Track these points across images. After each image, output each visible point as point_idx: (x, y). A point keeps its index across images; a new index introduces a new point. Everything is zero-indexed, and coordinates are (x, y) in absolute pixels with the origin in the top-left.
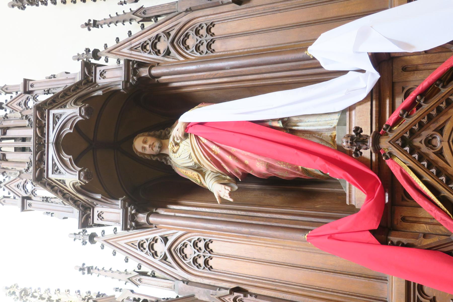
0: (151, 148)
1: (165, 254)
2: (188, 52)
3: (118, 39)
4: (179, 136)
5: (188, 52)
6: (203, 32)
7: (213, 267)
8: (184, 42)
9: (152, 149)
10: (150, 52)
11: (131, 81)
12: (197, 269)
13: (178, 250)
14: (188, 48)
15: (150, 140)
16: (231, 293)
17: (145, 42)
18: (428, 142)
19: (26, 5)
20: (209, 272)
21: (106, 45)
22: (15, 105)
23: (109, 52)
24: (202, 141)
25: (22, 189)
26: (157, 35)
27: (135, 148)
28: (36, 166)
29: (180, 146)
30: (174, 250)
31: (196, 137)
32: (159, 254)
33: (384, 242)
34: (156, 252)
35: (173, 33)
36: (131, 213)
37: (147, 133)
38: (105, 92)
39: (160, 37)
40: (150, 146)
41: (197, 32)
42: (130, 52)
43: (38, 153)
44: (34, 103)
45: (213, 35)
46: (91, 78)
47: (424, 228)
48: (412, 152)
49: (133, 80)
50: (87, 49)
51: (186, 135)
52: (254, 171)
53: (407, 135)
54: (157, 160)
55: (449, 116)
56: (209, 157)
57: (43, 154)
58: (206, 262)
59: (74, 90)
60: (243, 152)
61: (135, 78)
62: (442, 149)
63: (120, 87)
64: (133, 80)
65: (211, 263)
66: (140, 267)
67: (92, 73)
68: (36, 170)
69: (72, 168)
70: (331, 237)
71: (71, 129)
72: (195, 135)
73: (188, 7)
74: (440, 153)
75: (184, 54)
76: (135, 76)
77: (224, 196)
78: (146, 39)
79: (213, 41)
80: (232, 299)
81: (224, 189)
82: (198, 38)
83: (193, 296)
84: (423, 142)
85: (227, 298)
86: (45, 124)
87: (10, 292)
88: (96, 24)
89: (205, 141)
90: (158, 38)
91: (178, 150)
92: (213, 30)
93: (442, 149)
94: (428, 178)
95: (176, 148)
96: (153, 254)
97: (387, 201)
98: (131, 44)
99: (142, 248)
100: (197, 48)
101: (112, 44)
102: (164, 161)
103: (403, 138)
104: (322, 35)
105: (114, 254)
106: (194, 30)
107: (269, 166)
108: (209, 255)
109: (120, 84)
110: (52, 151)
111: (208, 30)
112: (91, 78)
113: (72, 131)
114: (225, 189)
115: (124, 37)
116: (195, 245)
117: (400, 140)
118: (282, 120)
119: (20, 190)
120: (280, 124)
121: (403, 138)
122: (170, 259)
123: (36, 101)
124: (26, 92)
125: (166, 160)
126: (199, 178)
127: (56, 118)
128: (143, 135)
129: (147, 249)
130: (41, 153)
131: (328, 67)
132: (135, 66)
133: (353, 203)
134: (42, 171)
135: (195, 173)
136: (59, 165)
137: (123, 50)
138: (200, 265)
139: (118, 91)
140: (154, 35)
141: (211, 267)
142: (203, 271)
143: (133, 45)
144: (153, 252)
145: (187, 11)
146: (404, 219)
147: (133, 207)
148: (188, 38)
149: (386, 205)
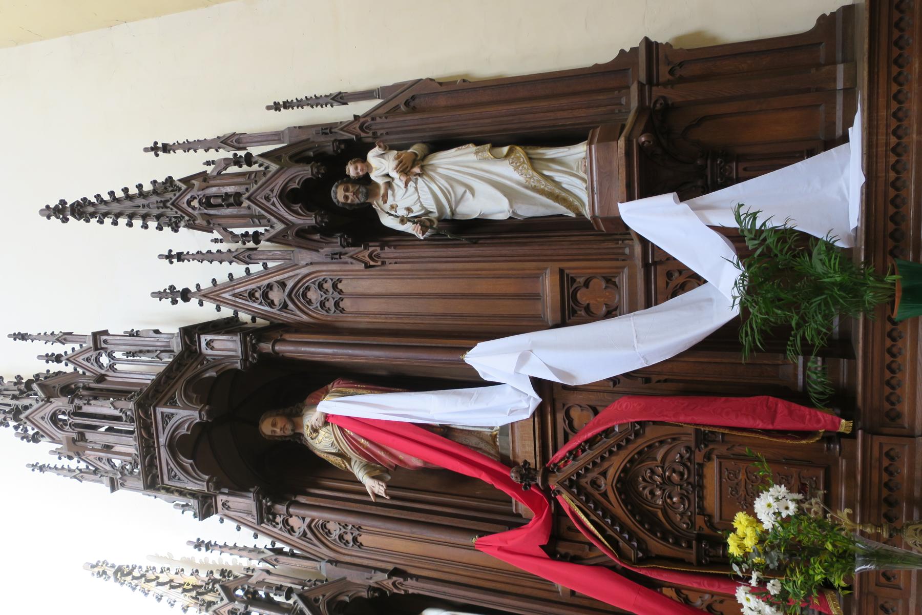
1: (304, 530)
2: (311, 307)
3: (214, 281)
5: (311, 307)
6: (328, 286)
7: (363, 544)
8: (304, 295)
10: (261, 302)
11: (250, 359)
12: (344, 546)
13: (320, 526)
14: (310, 302)
15: (280, 422)
16: (389, 578)
17: (253, 289)
18: (594, 483)
19: (69, 217)
20: (360, 550)
21: (198, 286)
22: (80, 359)
23: (205, 296)
24: (347, 433)
25: (107, 463)
26: (269, 284)
27: (262, 432)
28: (146, 472)
29: (319, 433)
30: (315, 526)
32: (296, 529)
34: (292, 528)
35: (290, 284)
36: (266, 505)
38: (219, 373)
39: (272, 285)
40: (281, 430)
41: (320, 286)
42: (233, 299)
43: (146, 457)
44: (110, 361)
45: (341, 292)
46: (194, 348)
48: (579, 494)
49: (253, 358)
51: (326, 423)
52: (409, 466)
53: (574, 478)
56: (358, 451)
57: (153, 458)
58: (355, 540)
59: (177, 369)
61: (255, 355)
62: (606, 490)
63: (238, 366)
64: (253, 358)
65: (360, 539)
66: (273, 544)
67: (196, 341)
69: (194, 474)
71: (187, 430)
72: (338, 426)
73: (309, 261)
74: (605, 495)
75: (304, 309)
76: (255, 353)
77: (378, 492)
78: (254, 286)
80: (390, 584)
81: (377, 486)
82: (322, 293)
83: (344, 578)
84: (589, 482)
86: (152, 423)
87: (99, 572)
88: (180, 257)
90: (270, 287)
91: (317, 436)
92: (340, 286)
93: (606, 490)
95: (315, 435)
96: (288, 530)
98: (234, 289)
99: (274, 524)
100: (322, 304)
101: (206, 285)
103: (570, 480)
104: (479, 344)
105: (239, 529)
106: (317, 283)
108: (357, 532)
109: (237, 363)
110: (164, 454)
111: (335, 286)
112: (194, 348)
113: (189, 433)
114: (379, 485)
115: (222, 279)
117: (567, 481)
119: (104, 463)
122: (309, 535)
123: (113, 359)
124: (96, 347)
125: (301, 440)
126: (344, 463)
127: (167, 418)
128: (271, 416)
129: (281, 525)
130: (151, 457)
131: (487, 379)
132: (254, 342)
133: (520, 512)
135: (339, 459)
136: (177, 470)
137: (223, 295)
138: (347, 541)
139: (236, 370)
140: (266, 282)
141: (361, 544)
142: (352, 548)
143: (237, 291)
144: (289, 527)
145: (307, 265)
147: (268, 499)
148: (309, 290)
149: (553, 515)
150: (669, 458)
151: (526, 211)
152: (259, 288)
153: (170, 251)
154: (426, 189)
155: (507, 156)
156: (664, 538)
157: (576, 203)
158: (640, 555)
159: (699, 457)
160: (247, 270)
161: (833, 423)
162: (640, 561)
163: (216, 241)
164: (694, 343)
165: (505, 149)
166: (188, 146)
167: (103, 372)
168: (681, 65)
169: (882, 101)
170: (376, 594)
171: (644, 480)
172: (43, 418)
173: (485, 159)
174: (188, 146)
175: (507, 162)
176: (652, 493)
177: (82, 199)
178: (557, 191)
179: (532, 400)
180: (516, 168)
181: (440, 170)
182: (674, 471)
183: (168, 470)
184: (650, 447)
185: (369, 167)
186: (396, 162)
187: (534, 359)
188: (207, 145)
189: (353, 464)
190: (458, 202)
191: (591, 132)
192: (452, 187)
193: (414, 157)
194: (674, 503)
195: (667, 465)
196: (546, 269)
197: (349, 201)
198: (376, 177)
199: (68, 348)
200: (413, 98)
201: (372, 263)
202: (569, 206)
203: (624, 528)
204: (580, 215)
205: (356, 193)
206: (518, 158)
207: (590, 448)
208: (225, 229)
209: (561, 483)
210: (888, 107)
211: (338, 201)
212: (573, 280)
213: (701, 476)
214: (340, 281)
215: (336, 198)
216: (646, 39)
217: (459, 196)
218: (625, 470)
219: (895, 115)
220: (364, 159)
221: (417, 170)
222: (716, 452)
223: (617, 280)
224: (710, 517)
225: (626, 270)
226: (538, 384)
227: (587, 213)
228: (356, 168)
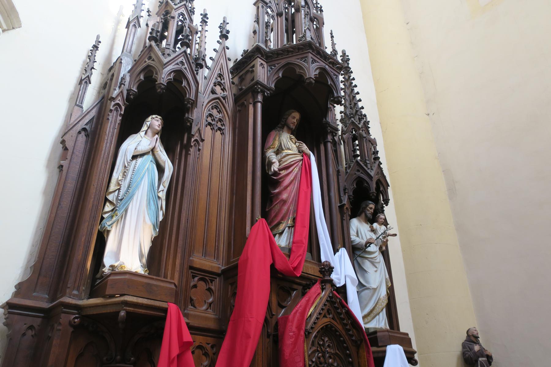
0: (293, 122)
4: (303, 148)
9: (293, 123)
12: (206, 115)
28: (317, 48)
37: (299, 123)
43: (323, 53)
50: (229, 32)
55: (339, 324)
57: (321, 57)
58: (210, 124)
68: (316, 47)
80: (197, 138)
85: (197, 134)
91: (292, 142)
97: (279, 275)
107: (284, 202)
134: (313, 50)
177: (351, 71)
211: (370, 204)
215: (372, 204)
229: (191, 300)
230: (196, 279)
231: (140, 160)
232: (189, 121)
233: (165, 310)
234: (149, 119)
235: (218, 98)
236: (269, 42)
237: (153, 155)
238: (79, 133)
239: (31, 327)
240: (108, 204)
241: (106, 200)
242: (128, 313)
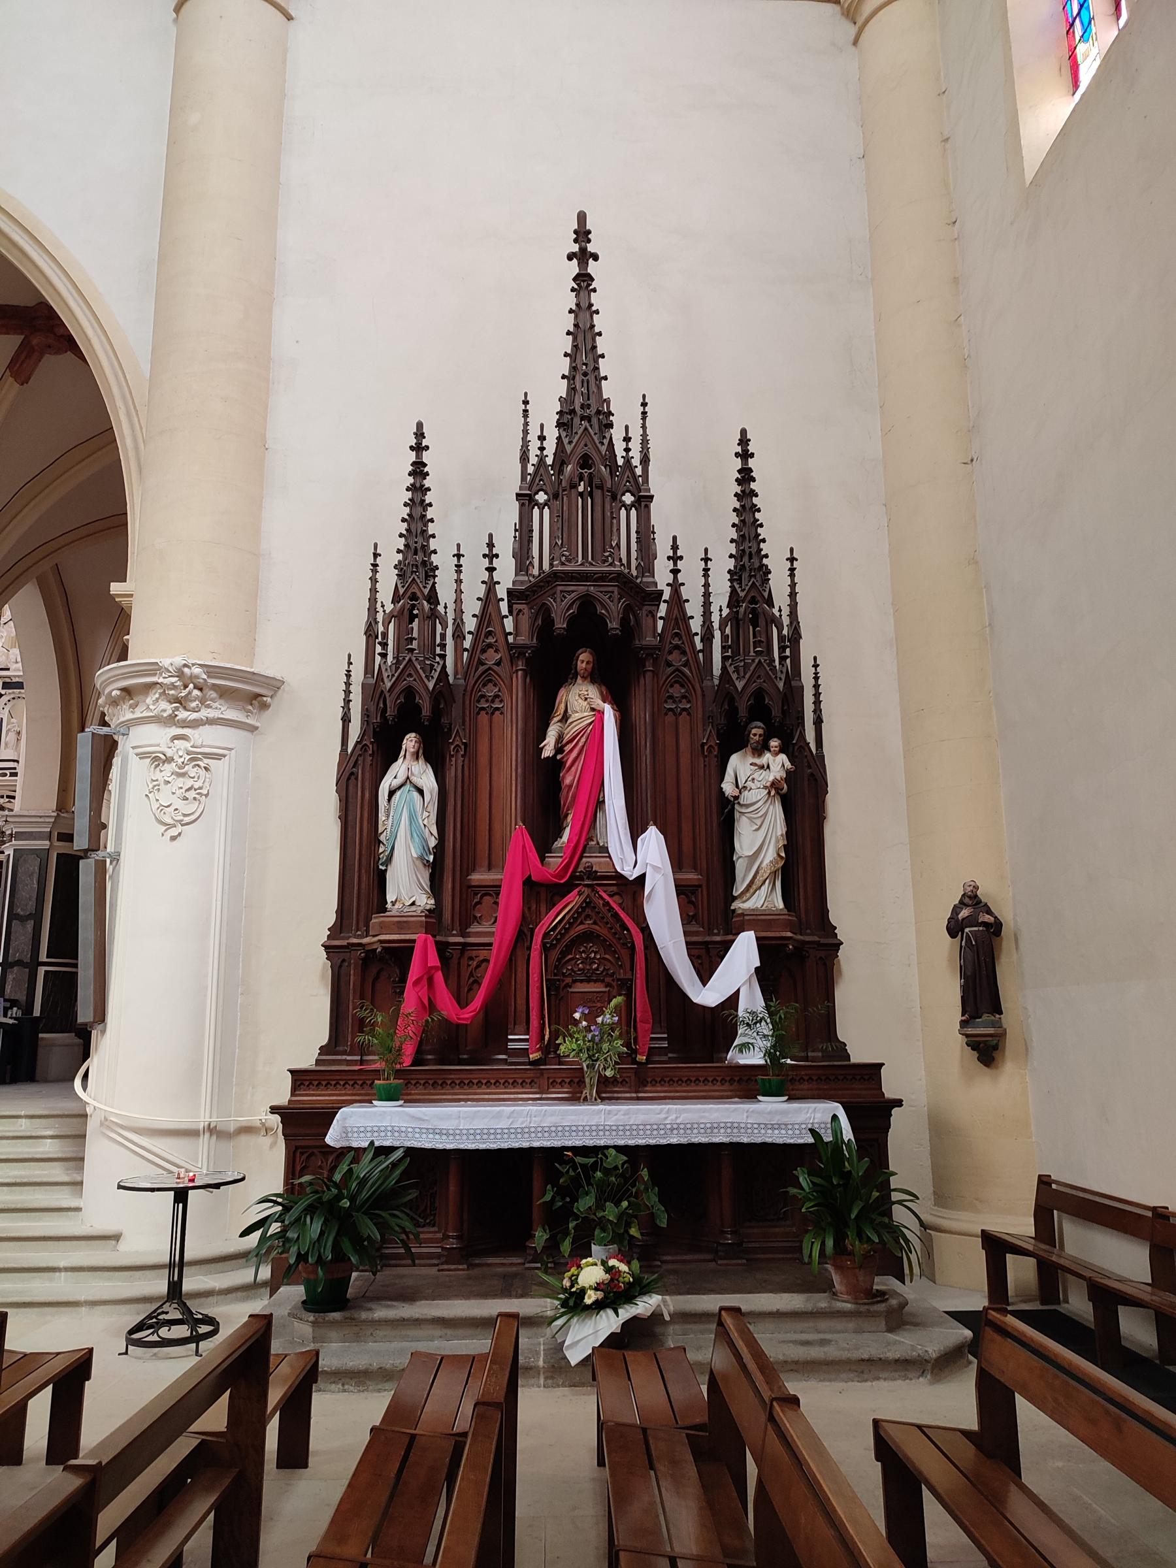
14: (672, 686)
18: (588, 917)
31: (592, 722)
33: (524, 883)
35: (686, 670)
41: (684, 697)
45: (680, 714)
47: (534, 907)
49: (643, 654)
54: (572, 670)
60: (580, 765)
64: (643, 654)
65: (483, 713)
70: (524, 846)
78: (684, 638)
79: (675, 714)
83: (455, 702)
85: (458, 738)
89: (588, 731)
90: (684, 653)
92: (684, 713)
94: (567, 918)
102: (571, 676)
103: (590, 902)
110: (582, 589)
116: (497, 696)
118: (604, 801)
120: (601, 799)
121: (590, 902)
122: (481, 669)
133: (546, 859)
140: (688, 651)
146: (538, 893)
150: (606, 962)
151: (740, 866)
152: (683, 643)
153: (596, 257)
154: (759, 798)
155: (779, 855)
156: (559, 960)
157: (745, 898)
158: (548, 945)
159: (608, 980)
160: (697, 634)
161: (644, 1052)
162: (544, 944)
163: (721, 610)
164: (674, 977)
165: (783, 854)
166: (793, 595)
167: (619, 497)
168: (825, 964)
169: (810, 1072)
170: (446, 730)
171: (591, 947)
172: (586, 445)
173: (777, 841)
174: (793, 595)
175: (775, 855)
176: (584, 951)
178: (754, 887)
179: (631, 874)
180: (771, 862)
181: (771, 807)
182: (598, 965)
183: (568, 592)
184: (615, 951)
185: (776, 754)
186: (779, 779)
187: (659, 876)
188: (793, 614)
189: (559, 724)
190: (748, 818)
191: (794, 914)
192: (761, 817)
193: (781, 787)
194: (578, 965)
195: (602, 961)
196: (701, 875)
197: (751, 736)
198: (768, 759)
199: (636, 462)
200: (816, 780)
201: (706, 747)
202: (743, 893)
203: (563, 935)
204: (734, 899)
205: (758, 742)
206: (777, 863)
207: (612, 915)
208: (730, 620)
209: (588, 896)
210: (806, 1075)
212: (693, 893)
213: (595, 981)
214: (689, 714)
216: (842, 943)
217: (754, 820)
218: (598, 936)
219: (802, 1078)
220: (781, 751)
221: (773, 793)
222: (611, 990)
223: (694, 923)
224: (570, 987)
225: (702, 929)
226: (642, 878)
227: (736, 905)
228: (776, 747)
229: (475, 917)
230: (479, 895)
231: (398, 794)
232: (446, 726)
233: (414, 941)
234: (405, 741)
235: (490, 669)
236: (530, 568)
237: (411, 782)
238: (349, 779)
239: (344, 961)
240: (381, 845)
241: (380, 842)
242: (384, 948)
